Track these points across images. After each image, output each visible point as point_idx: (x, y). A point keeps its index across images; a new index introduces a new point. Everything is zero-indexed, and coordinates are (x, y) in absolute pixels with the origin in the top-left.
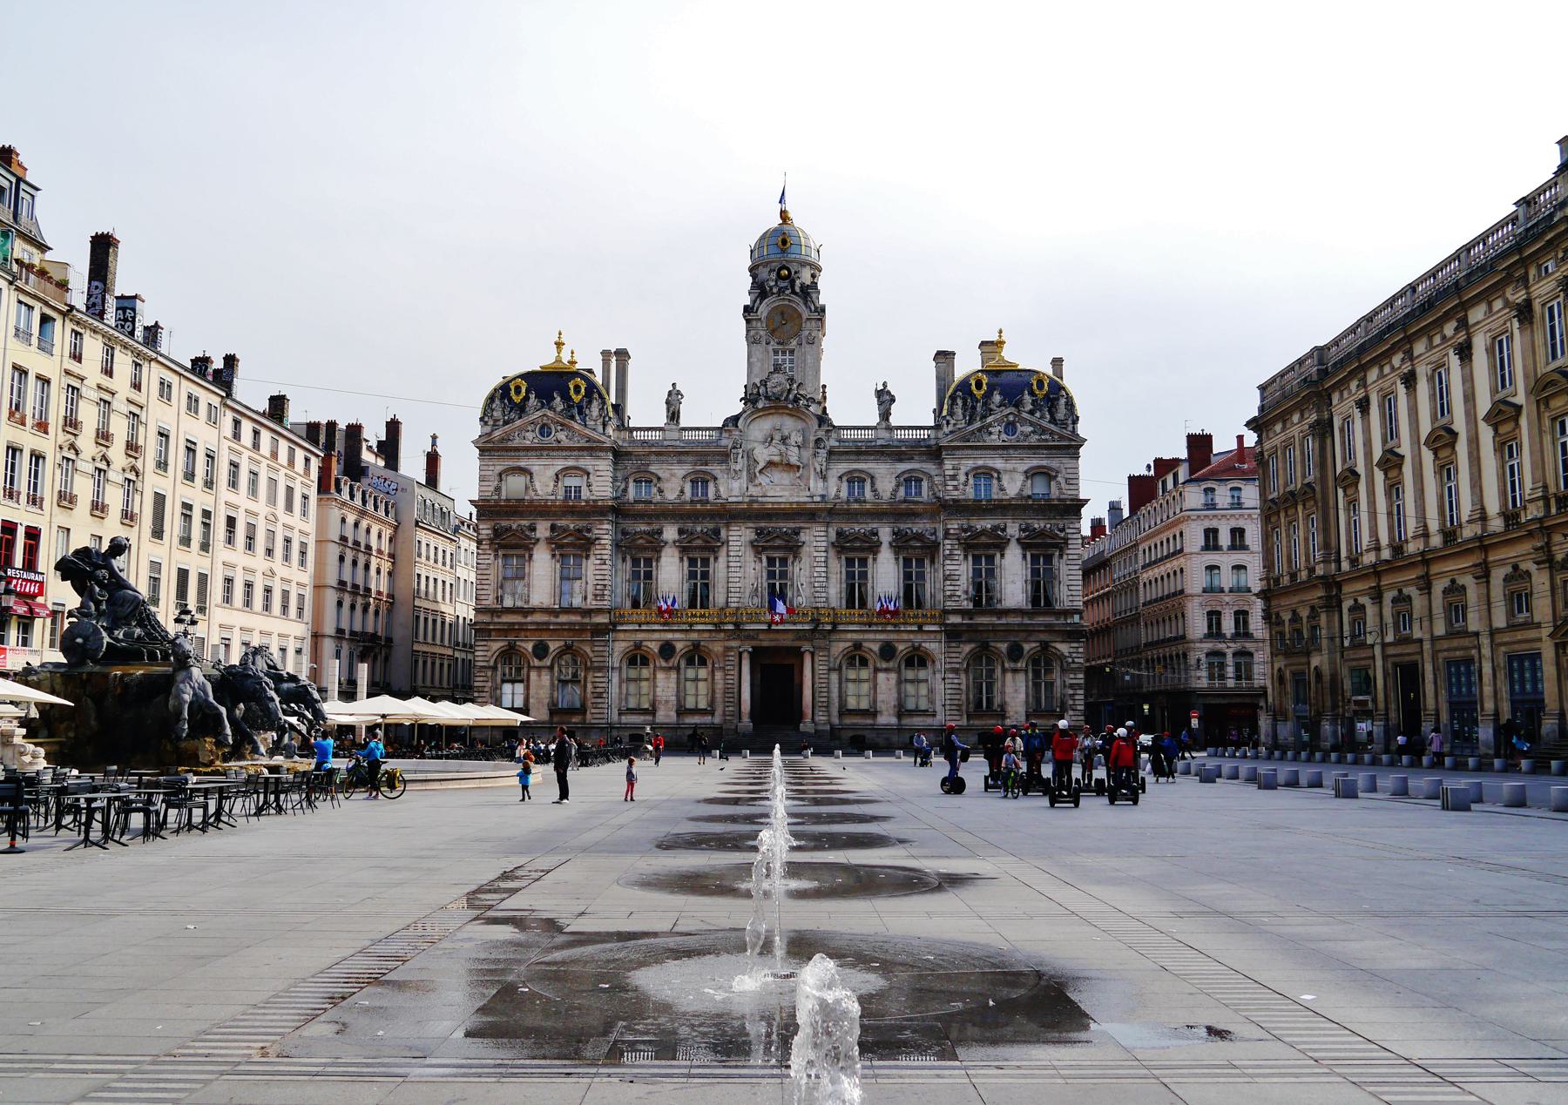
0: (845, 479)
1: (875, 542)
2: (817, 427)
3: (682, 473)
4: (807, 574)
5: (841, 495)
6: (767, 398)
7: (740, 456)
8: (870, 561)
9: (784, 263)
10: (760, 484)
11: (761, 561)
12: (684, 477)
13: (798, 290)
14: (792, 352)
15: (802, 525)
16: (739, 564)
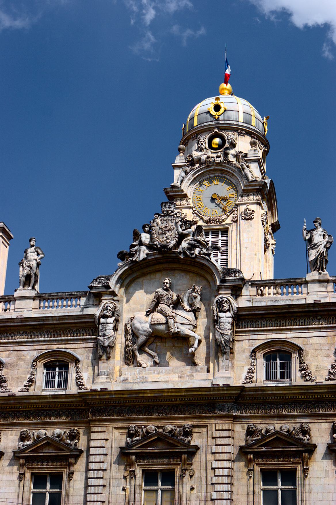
0: (260, 354)
1: (304, 445)
2: (218, 283)
3: (35, 354)
4: (203, 494)
5: (255, 378)
6: (149, 247)
7: (111, 326)
8: (299, 474)
9: (216, 130)
10: (140, 365)
11: (132, 475)
12: (35, 361)
13: (231, 158)
14: (225, 232)
15: (196, 422)
16: (101, 482)
